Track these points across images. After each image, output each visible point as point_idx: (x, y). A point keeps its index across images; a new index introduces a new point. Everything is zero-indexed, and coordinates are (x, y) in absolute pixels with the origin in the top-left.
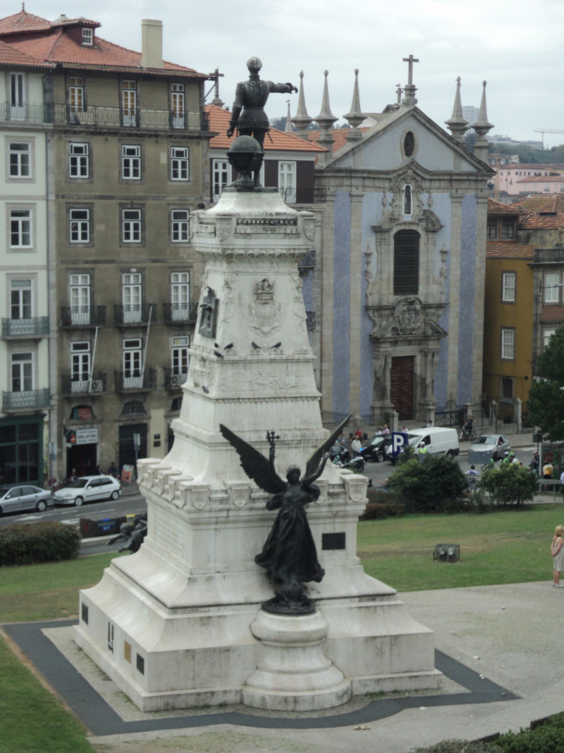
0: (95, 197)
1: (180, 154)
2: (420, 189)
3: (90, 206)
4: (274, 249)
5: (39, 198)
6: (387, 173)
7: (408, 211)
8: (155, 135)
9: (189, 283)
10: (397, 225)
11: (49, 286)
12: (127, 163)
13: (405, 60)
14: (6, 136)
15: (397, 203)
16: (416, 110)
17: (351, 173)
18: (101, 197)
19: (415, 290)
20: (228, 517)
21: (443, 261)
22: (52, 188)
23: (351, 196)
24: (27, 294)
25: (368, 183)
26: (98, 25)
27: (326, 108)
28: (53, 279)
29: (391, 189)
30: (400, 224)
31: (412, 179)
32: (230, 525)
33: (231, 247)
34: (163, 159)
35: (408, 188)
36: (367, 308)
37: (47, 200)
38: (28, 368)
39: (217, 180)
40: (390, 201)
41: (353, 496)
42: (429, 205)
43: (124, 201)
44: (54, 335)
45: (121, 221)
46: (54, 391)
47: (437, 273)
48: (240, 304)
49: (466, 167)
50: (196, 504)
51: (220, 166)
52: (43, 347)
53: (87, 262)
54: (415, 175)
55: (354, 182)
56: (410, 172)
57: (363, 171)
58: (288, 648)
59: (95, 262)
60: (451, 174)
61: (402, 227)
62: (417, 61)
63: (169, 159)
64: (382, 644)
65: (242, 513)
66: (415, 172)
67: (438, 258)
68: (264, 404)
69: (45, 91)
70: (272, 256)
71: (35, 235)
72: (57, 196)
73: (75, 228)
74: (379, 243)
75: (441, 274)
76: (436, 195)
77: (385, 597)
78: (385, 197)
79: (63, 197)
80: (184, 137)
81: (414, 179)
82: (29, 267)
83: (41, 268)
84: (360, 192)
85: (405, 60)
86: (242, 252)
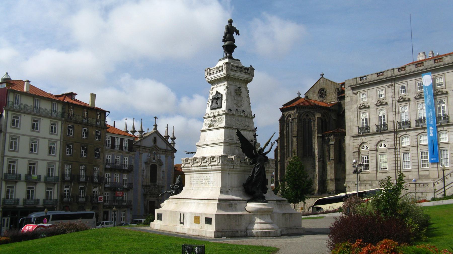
0: (74, 142)
1: (98, 132)
2: (157, 153)
3: (73, 144)
4: (242, 78)
5: (58, 140)
6: (149, 147)
7: (154, 159)
8: (92, 126)
9: (99, 171)
11: (59, 167)
12: (84, 133)
13: (154, 118)
14: (50, 120)
15: (152, 156)
16: (157, 131)
17: (140, 146)
18: (76, 142)
19: (156, 182)
20: (233, 168)
21: (163, 174)
22: (62, 138)
23: (139, 153)
24: (52, 169)
25: (144, 150)
26: (77, 94)
28: (60, 165)
29: (150, 152)
32: (233, 172)
33: (229, 74)
34: (94, 133)
35: (154, 152)
36: (143, 186)
37: (61, 141)
38: (51, 192)
39: (107, 142)
41: (271, 165)
43: (82, 144)
44: (59, 183)
45: (81, 150)
46: (58, 200)
47: (161, 177)
48: (231, 96)
49: (169, 148)
50: (224, 162)
51: (108, 138)
52: (56, 186)
53: (70, 161)
55: (141, 149)
57: (143, 146)
58: (262, 214)
59: (72, 161)
60: (165, 150)
61: (153, 164)
62: (157, 118)
63: (95, 133)
64: (287, 216)
66: (156, 148)
67: (162, 173)
69: (62, 109)
70: (241, 80)
71: (56, 151)
72: (63, 140)
73: (68, 150)
74: (147, 167)
76: (161, 155)
77: (284, 201)
79: (65, 141)
80: (100, 128)
81: (156, 150)
82: (54, 161)
83: (57, 161)
84: (142, 152)
85: (154, 118)
86: (232, 76)
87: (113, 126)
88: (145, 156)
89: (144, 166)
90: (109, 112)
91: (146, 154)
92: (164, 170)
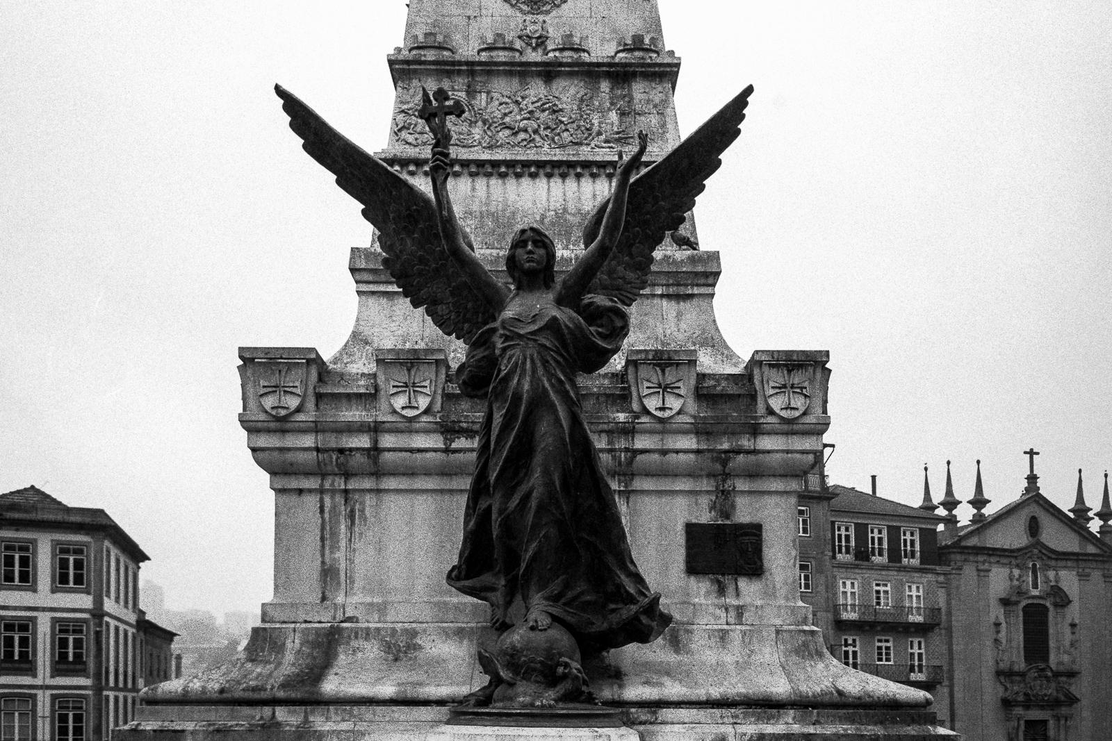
7: (1035, 586)
10: (1025, 599)
21: (1073, 633)
27: (949, 492)
29: (1017, 566)
30: (1029, 598)
31: (1038, 558)
35: (1034, 565)
40: (1017, 576)
42: (1057, 581)
47: (1067, 643)
54: (1040, 555)
55: (981, 558)
56: (1036, 551)
61: (1030, 601)
65: (420, 441)
66: (1040, 551)
67: (1068, 630)
68: (525, 181)
75: (1072, 645)
76: (1062, 573)
78: (1011, 572)
87: (871, 493)
88: (999, 579)
89: (997, 612)
90: (833, 446)
91: (1004, 572)
92: (1077, 621)
